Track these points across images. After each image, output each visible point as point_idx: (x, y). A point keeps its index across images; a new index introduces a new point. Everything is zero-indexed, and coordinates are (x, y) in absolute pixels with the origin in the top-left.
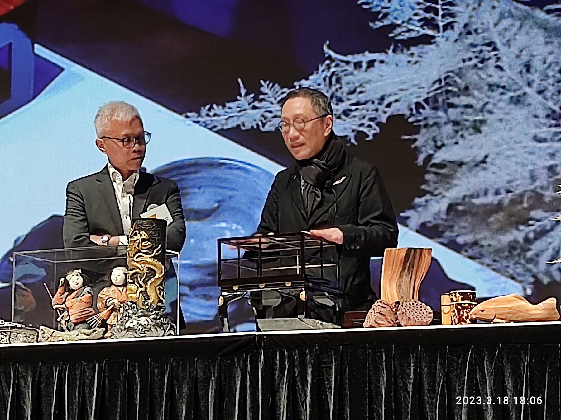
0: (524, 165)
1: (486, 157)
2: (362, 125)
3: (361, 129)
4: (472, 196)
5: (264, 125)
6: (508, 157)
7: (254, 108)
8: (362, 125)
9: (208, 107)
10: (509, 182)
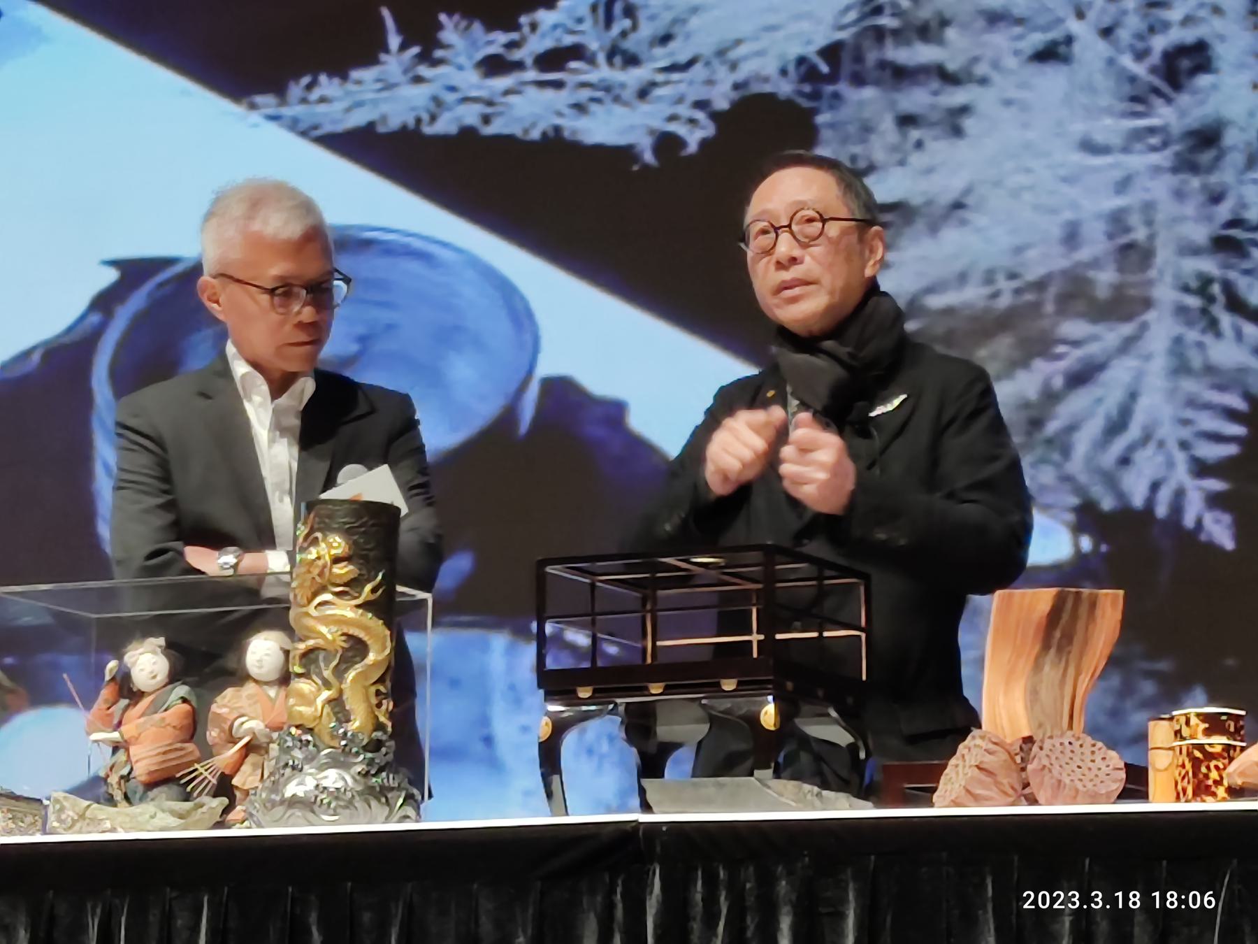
0: (1053, 211)
1: (968, 191)
2: (673, 118)
3: (673, 127)
4: (930, 290)
5: (433, 118)
6: (1016, 193)
7: (418, 80)
8: (673, 118)
9: (306, 80)
10: (1019, 250)
